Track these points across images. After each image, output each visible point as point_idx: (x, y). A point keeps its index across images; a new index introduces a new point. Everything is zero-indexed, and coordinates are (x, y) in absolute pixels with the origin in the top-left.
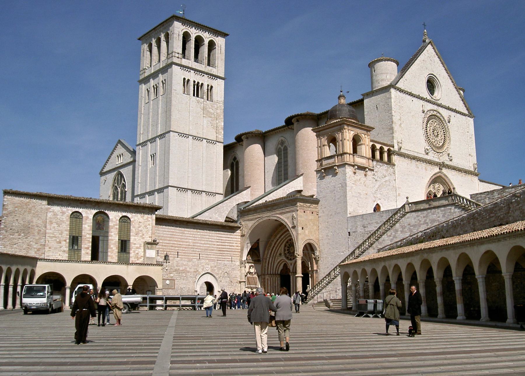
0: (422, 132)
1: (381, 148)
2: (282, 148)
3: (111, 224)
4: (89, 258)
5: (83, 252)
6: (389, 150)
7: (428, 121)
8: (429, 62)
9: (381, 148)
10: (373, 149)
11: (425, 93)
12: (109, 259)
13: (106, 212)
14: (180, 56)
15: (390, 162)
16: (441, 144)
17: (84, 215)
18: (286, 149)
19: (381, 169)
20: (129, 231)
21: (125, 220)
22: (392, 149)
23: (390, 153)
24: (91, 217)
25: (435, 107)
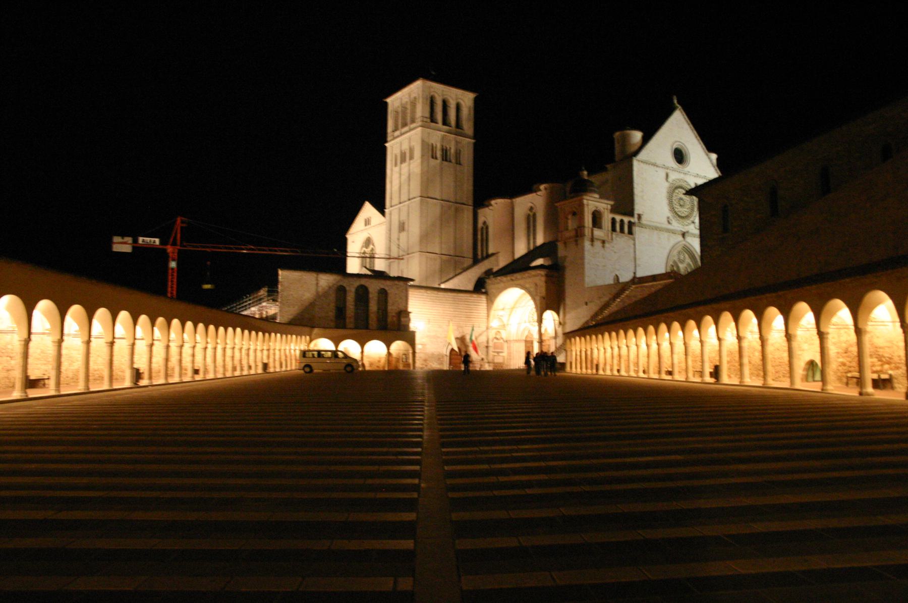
0: (665, 202)
1: (622, 221)
2: (531, 214)
3: (371, 296)
4: (352, 325)
5: (347, 320)
6: (630, 222)
7: (674, 190)
8: (678, 129)
9: (622, 221)
10: (613, 220)
11: (671, 162)
12: (370, 327)
13: (367, 285)
14: (429, 120)
15: (630, 232)
16: (687, 214)
17: (347, 288)
18: (534, 215)
19: (621, 241)
20: (386, 301)
21: (383, 293)
22: (632, 220)
23: (631, 224)
24: (353, 290)
25: (681, 176)
